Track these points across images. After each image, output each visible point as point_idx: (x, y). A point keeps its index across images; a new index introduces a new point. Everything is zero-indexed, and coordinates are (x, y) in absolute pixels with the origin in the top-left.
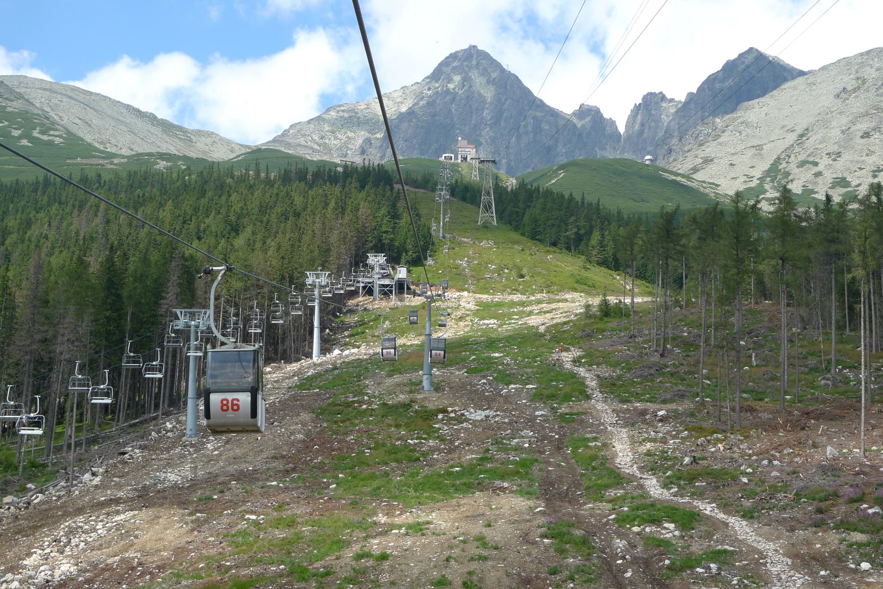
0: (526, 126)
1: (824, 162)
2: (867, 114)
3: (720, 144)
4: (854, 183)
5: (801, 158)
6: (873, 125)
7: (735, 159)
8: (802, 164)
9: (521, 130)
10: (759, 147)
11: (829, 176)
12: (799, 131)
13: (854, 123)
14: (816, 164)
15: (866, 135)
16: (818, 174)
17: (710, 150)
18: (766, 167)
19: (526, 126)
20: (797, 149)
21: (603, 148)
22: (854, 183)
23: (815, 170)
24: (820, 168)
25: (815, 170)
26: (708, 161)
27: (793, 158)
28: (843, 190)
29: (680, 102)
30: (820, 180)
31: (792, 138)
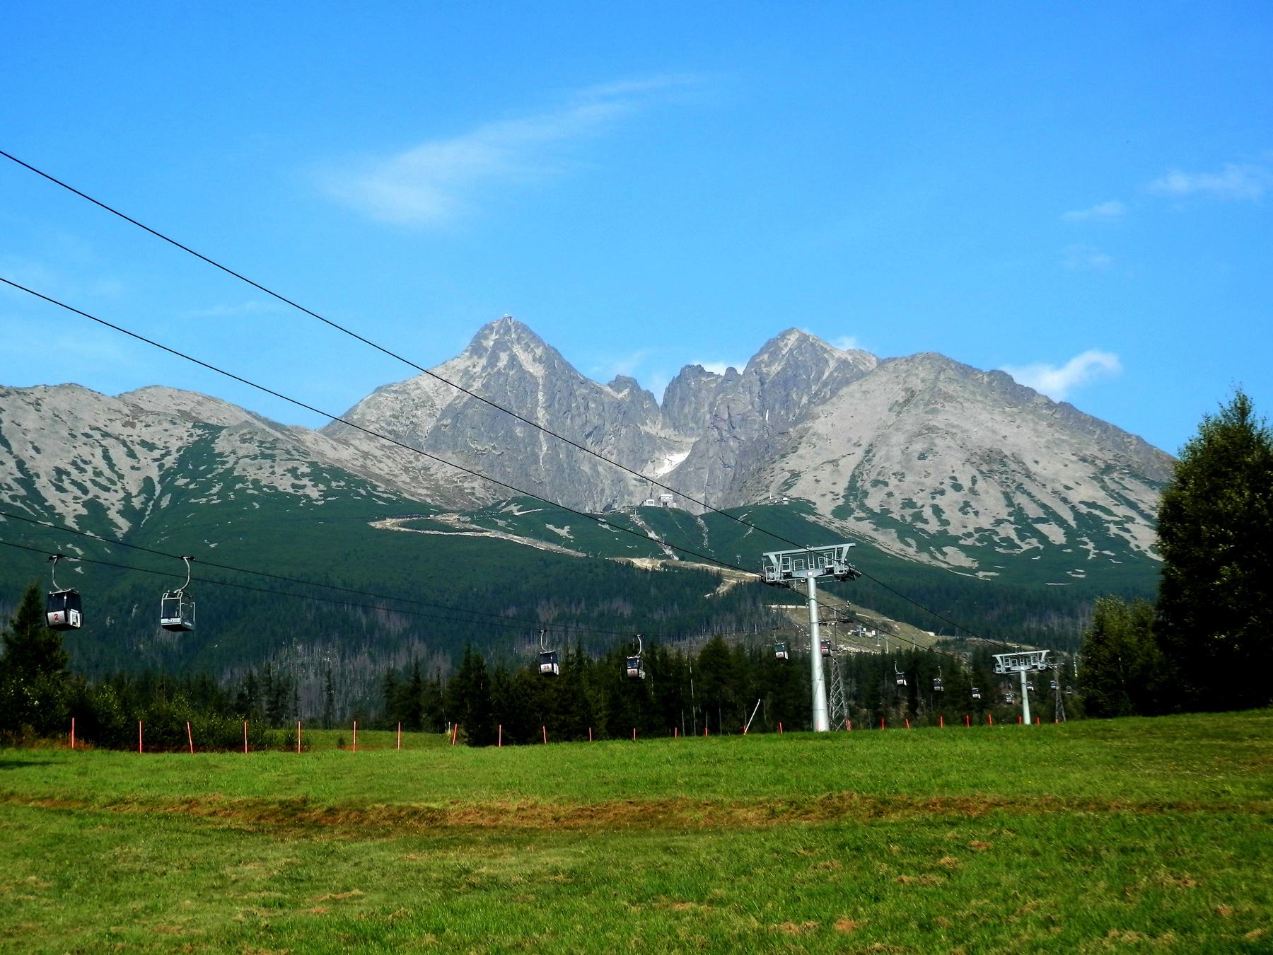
0: (578, 408)
1: (893, 482)
2: (920, 434)
3: (801, 457)
4: (919, 504)
5: (873, 476)
6: (926, 446)
7: (821, 475)
8: (876, 483)
9: (575, 412)
11: (898, 498)
12: (865, 447)
13: (911, 442)
14: (886, 484)
15: (922, 457)
16: (890, 494)
17: (792, 463)
18: (846, 485)
19: (578, 408)
21: (644, 424)
22: (919, 504)
23: (887, 490)
24: (890, 489)
25: (887, 490)
26: (795, 475)
27: (865, 477)
28: (911, 511)
29: (719, 376)
31: (860, 453)
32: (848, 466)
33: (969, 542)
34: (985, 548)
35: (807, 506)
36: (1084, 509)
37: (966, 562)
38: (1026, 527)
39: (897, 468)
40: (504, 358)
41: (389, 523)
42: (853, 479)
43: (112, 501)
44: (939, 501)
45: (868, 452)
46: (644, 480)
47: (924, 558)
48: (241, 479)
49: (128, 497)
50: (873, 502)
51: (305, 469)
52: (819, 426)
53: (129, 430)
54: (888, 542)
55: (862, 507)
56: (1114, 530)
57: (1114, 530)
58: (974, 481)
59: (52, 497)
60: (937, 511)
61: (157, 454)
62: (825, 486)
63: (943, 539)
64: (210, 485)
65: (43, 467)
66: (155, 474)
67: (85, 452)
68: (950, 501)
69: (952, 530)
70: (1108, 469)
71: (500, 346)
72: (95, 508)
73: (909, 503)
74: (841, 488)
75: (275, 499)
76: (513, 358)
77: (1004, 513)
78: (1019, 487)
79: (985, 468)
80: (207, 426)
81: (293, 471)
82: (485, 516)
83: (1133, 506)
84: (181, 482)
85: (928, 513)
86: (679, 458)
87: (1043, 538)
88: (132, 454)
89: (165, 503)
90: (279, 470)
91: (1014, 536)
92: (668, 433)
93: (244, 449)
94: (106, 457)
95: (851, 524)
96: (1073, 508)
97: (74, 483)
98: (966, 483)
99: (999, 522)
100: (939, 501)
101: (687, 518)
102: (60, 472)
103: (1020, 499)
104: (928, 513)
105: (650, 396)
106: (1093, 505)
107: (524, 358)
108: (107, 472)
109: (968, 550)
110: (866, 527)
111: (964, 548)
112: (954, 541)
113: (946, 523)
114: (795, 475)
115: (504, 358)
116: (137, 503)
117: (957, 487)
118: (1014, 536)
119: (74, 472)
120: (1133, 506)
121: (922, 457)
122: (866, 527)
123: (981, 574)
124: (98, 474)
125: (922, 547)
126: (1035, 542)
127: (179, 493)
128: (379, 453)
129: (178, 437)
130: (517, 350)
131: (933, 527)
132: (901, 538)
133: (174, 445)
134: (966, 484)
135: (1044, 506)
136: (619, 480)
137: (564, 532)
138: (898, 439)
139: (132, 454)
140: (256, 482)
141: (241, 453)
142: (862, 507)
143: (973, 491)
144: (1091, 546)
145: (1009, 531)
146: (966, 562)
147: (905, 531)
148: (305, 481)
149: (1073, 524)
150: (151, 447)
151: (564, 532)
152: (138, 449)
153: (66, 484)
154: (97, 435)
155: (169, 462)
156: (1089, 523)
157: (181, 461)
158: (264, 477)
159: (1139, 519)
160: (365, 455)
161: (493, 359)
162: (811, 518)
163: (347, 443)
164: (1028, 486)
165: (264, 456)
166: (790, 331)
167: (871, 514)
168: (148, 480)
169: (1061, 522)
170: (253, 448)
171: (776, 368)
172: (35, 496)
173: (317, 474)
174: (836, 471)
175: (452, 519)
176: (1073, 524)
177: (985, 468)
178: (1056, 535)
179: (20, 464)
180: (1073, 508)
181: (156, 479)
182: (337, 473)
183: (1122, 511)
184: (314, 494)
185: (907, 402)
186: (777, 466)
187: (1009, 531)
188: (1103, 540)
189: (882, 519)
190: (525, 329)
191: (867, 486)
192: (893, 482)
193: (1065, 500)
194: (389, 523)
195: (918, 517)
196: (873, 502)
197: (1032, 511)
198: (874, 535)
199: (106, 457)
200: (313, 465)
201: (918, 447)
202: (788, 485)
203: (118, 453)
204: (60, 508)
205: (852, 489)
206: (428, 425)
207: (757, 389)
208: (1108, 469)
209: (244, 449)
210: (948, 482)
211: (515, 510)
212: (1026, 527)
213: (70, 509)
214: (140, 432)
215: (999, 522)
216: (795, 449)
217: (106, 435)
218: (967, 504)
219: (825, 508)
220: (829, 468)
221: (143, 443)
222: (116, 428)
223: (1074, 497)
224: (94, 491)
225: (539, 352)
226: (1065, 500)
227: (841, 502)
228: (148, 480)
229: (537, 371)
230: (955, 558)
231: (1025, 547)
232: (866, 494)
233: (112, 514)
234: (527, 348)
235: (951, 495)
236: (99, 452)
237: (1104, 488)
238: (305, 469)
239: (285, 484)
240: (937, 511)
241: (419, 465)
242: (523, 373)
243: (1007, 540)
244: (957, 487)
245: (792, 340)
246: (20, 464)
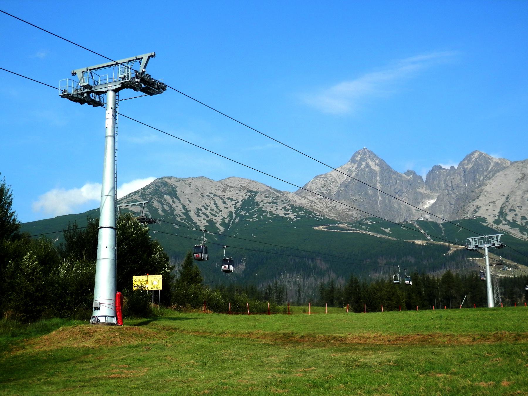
0: (393, 182)
1: (517, 210)
3: (480, 200)
5: (509, 207)
7: (488, 207)
8: (510, 210)
11: (520, 216)
12: (506, 196)
14: (515, 211)
16: (516, 215)
17: (477, 203)
19: (393, 182)
20: (507, 204)
21: (418, 188)
23: (515, 213)
24: (516, 212)
25: (515, 213)
26: (479, 207)
27: (506, 208)
30: (517, 217)
31: (504, 199)
32: (499, 204)
35: (483, 220)
39: (519, 204)
40: (364, 164)
41: (321, 228)
42: (502, 209)
43: (218, 220)
45: (507, 198)
46: (419, 210)
48: (265, 211)
49: (223, 218)
50: (510, 218)
51: (289, 207)
52: (488, 188)
53: (223, 194)
54: (516, 233)
55: (505, 220)
59: (195, 219)
61: (234, 202)
62: (490, 211)
65: (192, 208)
66: (233, 210)
67: (207, 202)
71: (362, 159)
72: (212, 223)
74: (497, 212)
75: (278, 218)
76: (367, 165)
80: (252, 192)
82: (357, 224)
84: (243, 213)
86: (432, 201)
88: (224, 203)
89: (237, 221)
90: (279, 208)
92: (428, 192)
93: (266, 200)
94: (215, 204)
95: (501, 226)
97: (203, 213)
101: (436, 225)
102: (198, 210)
105: (421, 178)
107: (371, 164)
108: (215, 209)
110: (507, 228)
114: (479, 207)
115: (364, 164)
116: (226, 221)
119: (203, 210)
122: (507, 228)
124: (212, 210)
127: (242, 217)
128: (316, 201)
129: (242, 196)
130: (369, 161)
132: (521, 232)
133: (240, 199)
136: (409, 210)
137: (388, 230)
138: (519, 193)
139: (224, 203)
140: (270, 212)
141: (265, 202)
142: (505, 220)
148: (289, 212)
150: (232, 200)
151: (388, 230)
152: (227, 201)
153: (201, 214)
154: (212, 196)
155: (238, 205)
157: (243, 205)
160: (312, 202)
161: (360, 164)
162: (485, 224)
163: (304, 197)
165: (273, 203)
166: (475, 152)
167: (509, 223)
168: (231, 212)
170: (269, 200)
171: (470, 166)
172: (189, 219)
173: (294, 209)
174: (495, 206)
175: (345, 226)
179: (184, 207)
181: (234, 212)
182: (301, 209)
184: (292, 216)
185: (523, 178)
186: (471, 204)
189: (513, 224)
190: (372, 153)
191: (507, 211)
192: (517, 210)
194: (321, 228)
196: (510, 218)
198: (510, 230)
199: (215, 204)
200: (292, 206)
202: (475, 211)
203: (219, 202)
204: (198, 223)
205: (501, 213)
206: (335, 190)
207: (462, 174)
209: (266, 200)
211: (369, 222)
213: (202, 223)
214: (227, 194)
216: (478, 197)
217: (215, 195)
219: (490, 220)
220: (492, 204)
221: (229, 198)
222: (219, 193)
224: (211, 216)
225: (377, 161)
227: (497, 218)
228: (231, 212)
229: (377, 169)
232: (506, 215)
233: (218, 225)
234: (372, 160)
236: (212, 202)
238: (289, 207)
239: (281, 213)
241: (332, 205)
242: (371, 170)
245: (476, 155)
246: (184, 207)
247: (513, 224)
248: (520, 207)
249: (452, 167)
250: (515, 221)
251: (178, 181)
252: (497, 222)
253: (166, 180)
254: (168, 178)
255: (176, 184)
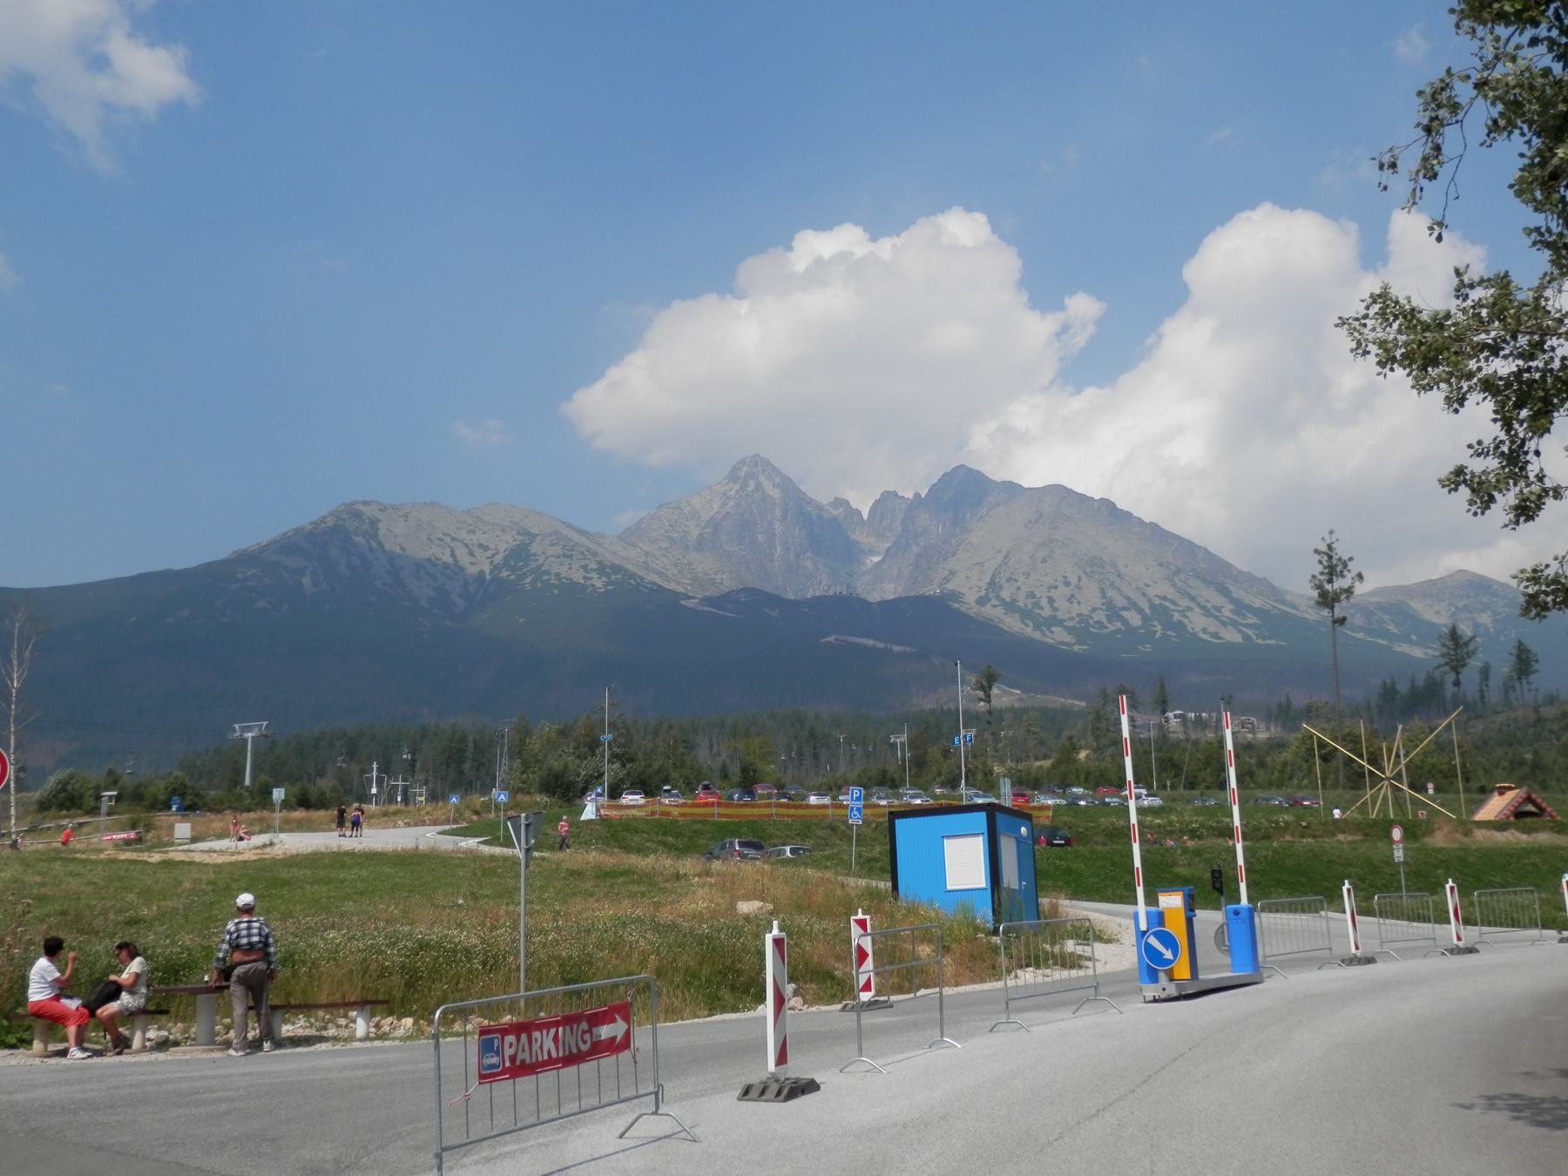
1: (1022, 579)
8: (1009, 580)
10: (981, 564)
15: (1044, 561)
26: (953, 573)
31: (1000, 557)
33: (1071, 624)
34: (1082, 630)
35: (956, 596)
36: (1157, 601)
37: (1067, 638)
38: (1113, 612)
40: (752, 485)
44: (1053, 593)
47: (1037, 635)
50: (1006, 594)
53: (471, 536)
55: (998, 597)
56: (1177, 616)
57: (1177, 616)
58: (1079, 579)
60: (1051, 601)
61: (489, 553)
63: (1054, 621)
64: (525, 576)
68: (1060, 594)
69: (1060, 615)
70: (1178, 572)
73: (1031, 595)
74: (984, 586)
75: (572, 587)
76: (759, 486)
77: (1097, 601)
78: (1112, 584)
79: (1088, 570)
80: (528, 534)
81: (585, 567)
83: (1193, 599)
85: (1044, 602)
86: (876, 559)
87: (1125, 621)
88: (471, 553)
91: (1104, 620)
96: (1149, 600)
98: (1074, 581)
99: (1094, 610)
100: (1053, 593)
103: (1110, 593)
104: (1044, 602)
105: (859, 513)
106: (1164, 598)
107: (767, 485)
109: (1069, 630)
111: (1067, 629)
112: (1060, 623)
113: (1056, 609)
114: (953, 573)
115: (752, 485)
116: (472, 589)
117: (1067, 584)
118: (1104, 620)
120: (1193, 599)
121: (1044, 561)
123: (1076, 648)
125: (1037, 627)
126: (1119, 624)
128: (657, 553)
129: (506, 542)
130: (762, 479)
131: (1047, 612)
133: (503, 547)
134: (1074, 581)
135: (1128, 599)
139: (471, 553)
140: (558, 575)
141: (549, 553)
143: (1078, 587)
144: (1159, 627)
145: (1101, 616)
146: (1067, 638)
147: (1026, 615)
148: (594, 575)
149: (1148, 611)
150: (486, 548)
152: (476, 550)
154: (448, 540)
155: (498, 559)
156: (1160, 611)
157: (506, 559)
158: (563, 571)
159: (1197, 609)
160: (647, 554)
161: (744, 485)
162: (956, 605)
163: (634, 545)
164: (1118, 583)
165: (565, 556)
169: (1139, 610)
170: (558, 550)
173: (602, 569)
176: (1148, 611)
177: (1088, 570)
178: (1135, 619)
180: (1149, 600)
181: (487, 572)
182: (616, 569)
183: (1185, 603)
184: (598, 583)
185: (1037, 521)
187: (1101, 616)
188: (1168, 624)
189: (1010, 607)
190: (769, 463)
192: (1022, 579)
193: (1144, 595)
195: (1037, 605)
197: (1120, 602)
198: (1002, 617)
200: (600, 563)
201: (1042, 554)
202: (947, 580)
205: (992, 584)
206: (695, 533)
208: (1178, 572)
210: (1061, 579)
212: (1113, 612)
215: (1094, 610)
216: (954, 554)
217: (454, 539)
218: (1072, 596)
219: (970, 597)
221: (481, 546)
222: (463, 535)
223: (1151, 592)
226: (1144, 595)
229: (776, 494)
230: (1059, 636)
231: (1111, 628)
232: (1001, 588)
235: (1062, 589)
236: (448, 552)
237: (1174, 586)
238: (594, 566)
239: (578, 577)
240: (1051, 601)
243: (1099, 622)
244: (1067, 584)
247: (1010, 607)
248: (1027, 575)
249: (917, 495)
250: (1014, 601)
251: (384, 509)
252: (982, 601)
253: (361, 507)
254: (365, 503)
255: (379, 515)
